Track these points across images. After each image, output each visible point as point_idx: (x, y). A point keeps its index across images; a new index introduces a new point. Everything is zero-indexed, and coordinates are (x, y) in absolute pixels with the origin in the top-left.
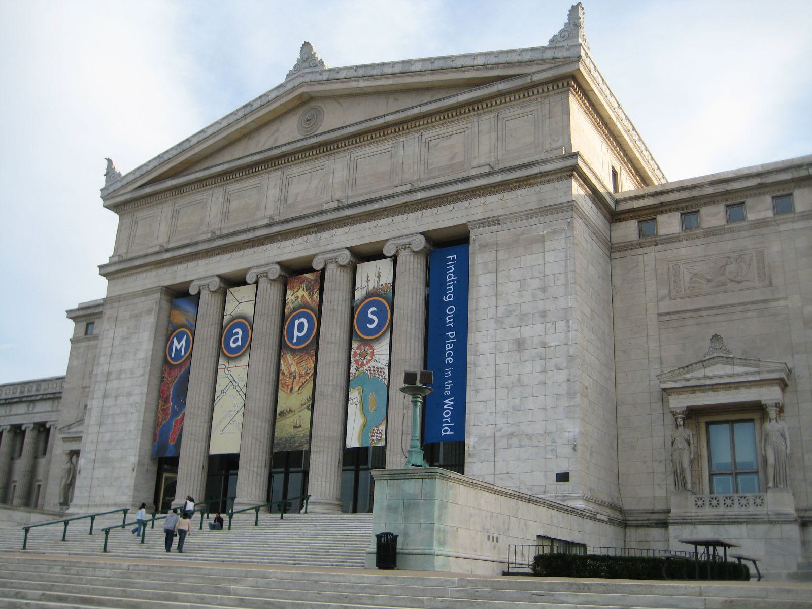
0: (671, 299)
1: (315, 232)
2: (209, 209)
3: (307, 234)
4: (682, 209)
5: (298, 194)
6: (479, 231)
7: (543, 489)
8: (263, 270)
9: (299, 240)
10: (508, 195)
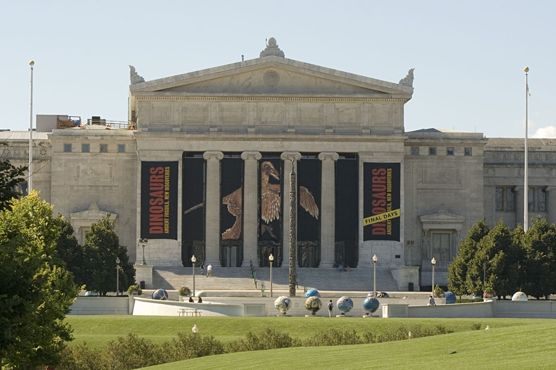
0: (422, 183)
1: (281, 141)
2: (209, 113)
3: (276, 141)
4: (430, 146)
5: (267, 118)
6: (364, 157)
7: (390, 261)
8: (250, 153)
9: (272, 142)
10: (376, 144)
